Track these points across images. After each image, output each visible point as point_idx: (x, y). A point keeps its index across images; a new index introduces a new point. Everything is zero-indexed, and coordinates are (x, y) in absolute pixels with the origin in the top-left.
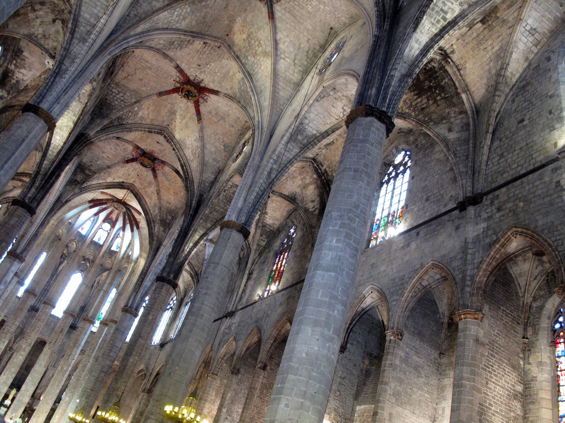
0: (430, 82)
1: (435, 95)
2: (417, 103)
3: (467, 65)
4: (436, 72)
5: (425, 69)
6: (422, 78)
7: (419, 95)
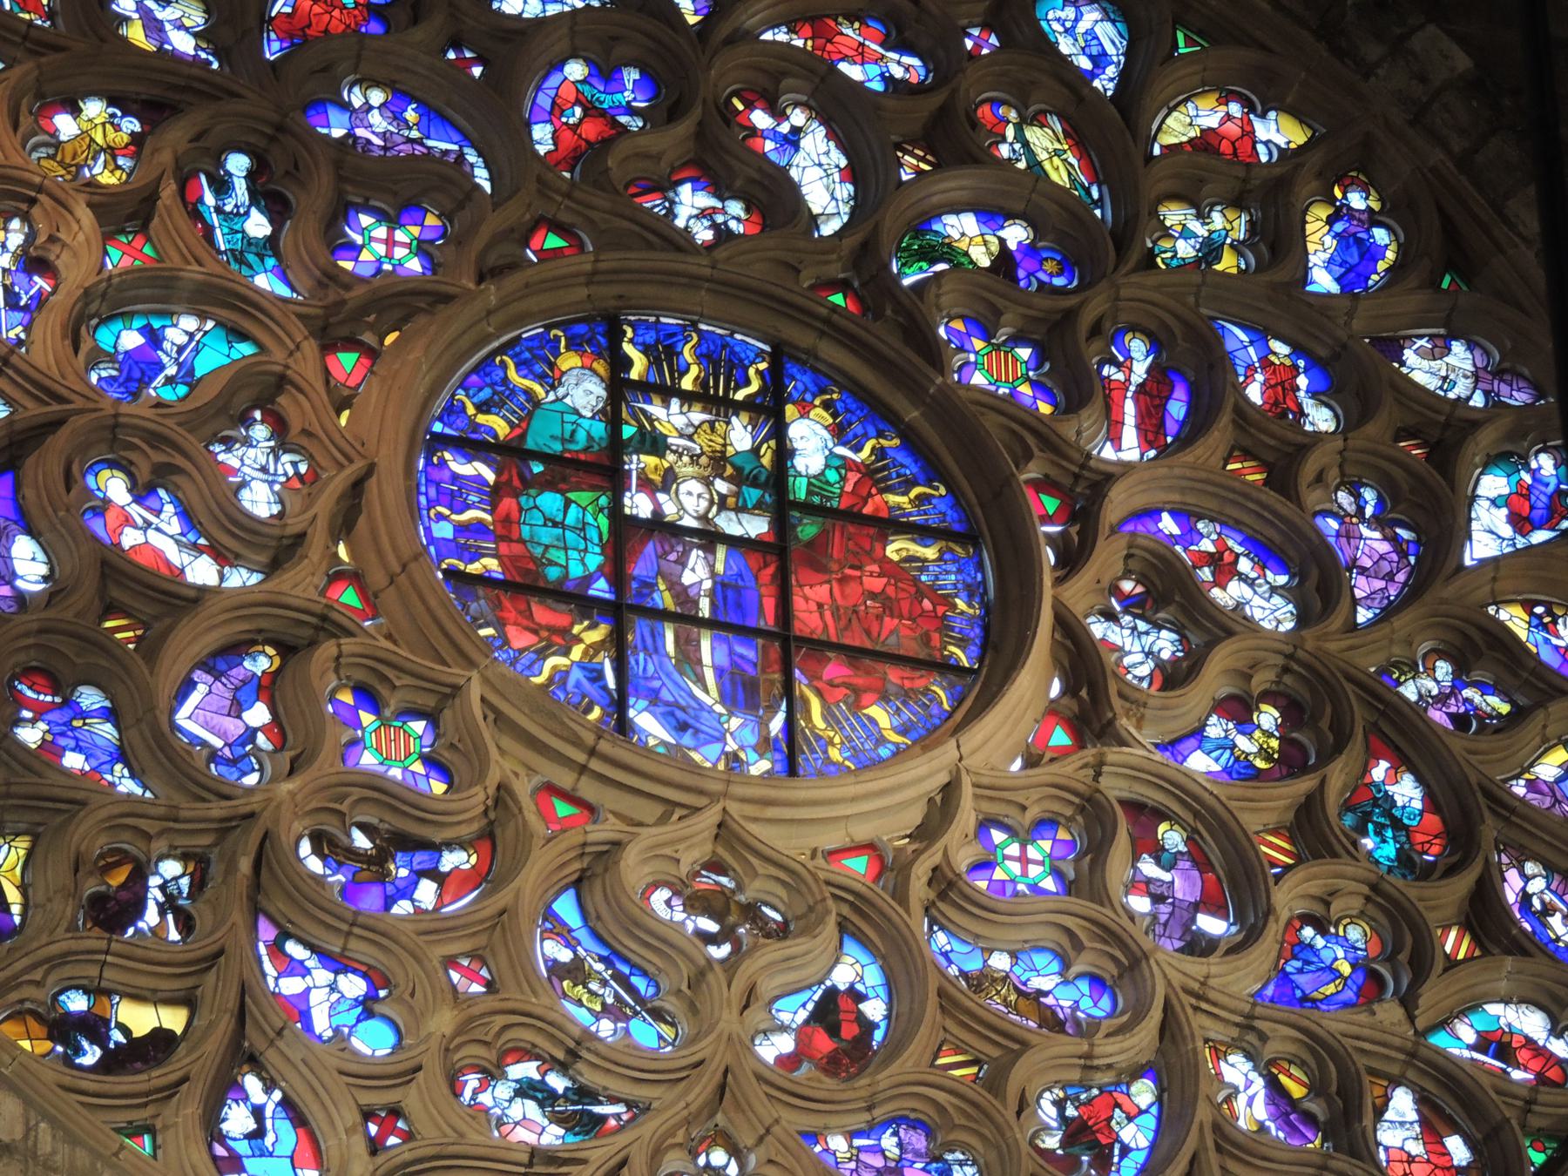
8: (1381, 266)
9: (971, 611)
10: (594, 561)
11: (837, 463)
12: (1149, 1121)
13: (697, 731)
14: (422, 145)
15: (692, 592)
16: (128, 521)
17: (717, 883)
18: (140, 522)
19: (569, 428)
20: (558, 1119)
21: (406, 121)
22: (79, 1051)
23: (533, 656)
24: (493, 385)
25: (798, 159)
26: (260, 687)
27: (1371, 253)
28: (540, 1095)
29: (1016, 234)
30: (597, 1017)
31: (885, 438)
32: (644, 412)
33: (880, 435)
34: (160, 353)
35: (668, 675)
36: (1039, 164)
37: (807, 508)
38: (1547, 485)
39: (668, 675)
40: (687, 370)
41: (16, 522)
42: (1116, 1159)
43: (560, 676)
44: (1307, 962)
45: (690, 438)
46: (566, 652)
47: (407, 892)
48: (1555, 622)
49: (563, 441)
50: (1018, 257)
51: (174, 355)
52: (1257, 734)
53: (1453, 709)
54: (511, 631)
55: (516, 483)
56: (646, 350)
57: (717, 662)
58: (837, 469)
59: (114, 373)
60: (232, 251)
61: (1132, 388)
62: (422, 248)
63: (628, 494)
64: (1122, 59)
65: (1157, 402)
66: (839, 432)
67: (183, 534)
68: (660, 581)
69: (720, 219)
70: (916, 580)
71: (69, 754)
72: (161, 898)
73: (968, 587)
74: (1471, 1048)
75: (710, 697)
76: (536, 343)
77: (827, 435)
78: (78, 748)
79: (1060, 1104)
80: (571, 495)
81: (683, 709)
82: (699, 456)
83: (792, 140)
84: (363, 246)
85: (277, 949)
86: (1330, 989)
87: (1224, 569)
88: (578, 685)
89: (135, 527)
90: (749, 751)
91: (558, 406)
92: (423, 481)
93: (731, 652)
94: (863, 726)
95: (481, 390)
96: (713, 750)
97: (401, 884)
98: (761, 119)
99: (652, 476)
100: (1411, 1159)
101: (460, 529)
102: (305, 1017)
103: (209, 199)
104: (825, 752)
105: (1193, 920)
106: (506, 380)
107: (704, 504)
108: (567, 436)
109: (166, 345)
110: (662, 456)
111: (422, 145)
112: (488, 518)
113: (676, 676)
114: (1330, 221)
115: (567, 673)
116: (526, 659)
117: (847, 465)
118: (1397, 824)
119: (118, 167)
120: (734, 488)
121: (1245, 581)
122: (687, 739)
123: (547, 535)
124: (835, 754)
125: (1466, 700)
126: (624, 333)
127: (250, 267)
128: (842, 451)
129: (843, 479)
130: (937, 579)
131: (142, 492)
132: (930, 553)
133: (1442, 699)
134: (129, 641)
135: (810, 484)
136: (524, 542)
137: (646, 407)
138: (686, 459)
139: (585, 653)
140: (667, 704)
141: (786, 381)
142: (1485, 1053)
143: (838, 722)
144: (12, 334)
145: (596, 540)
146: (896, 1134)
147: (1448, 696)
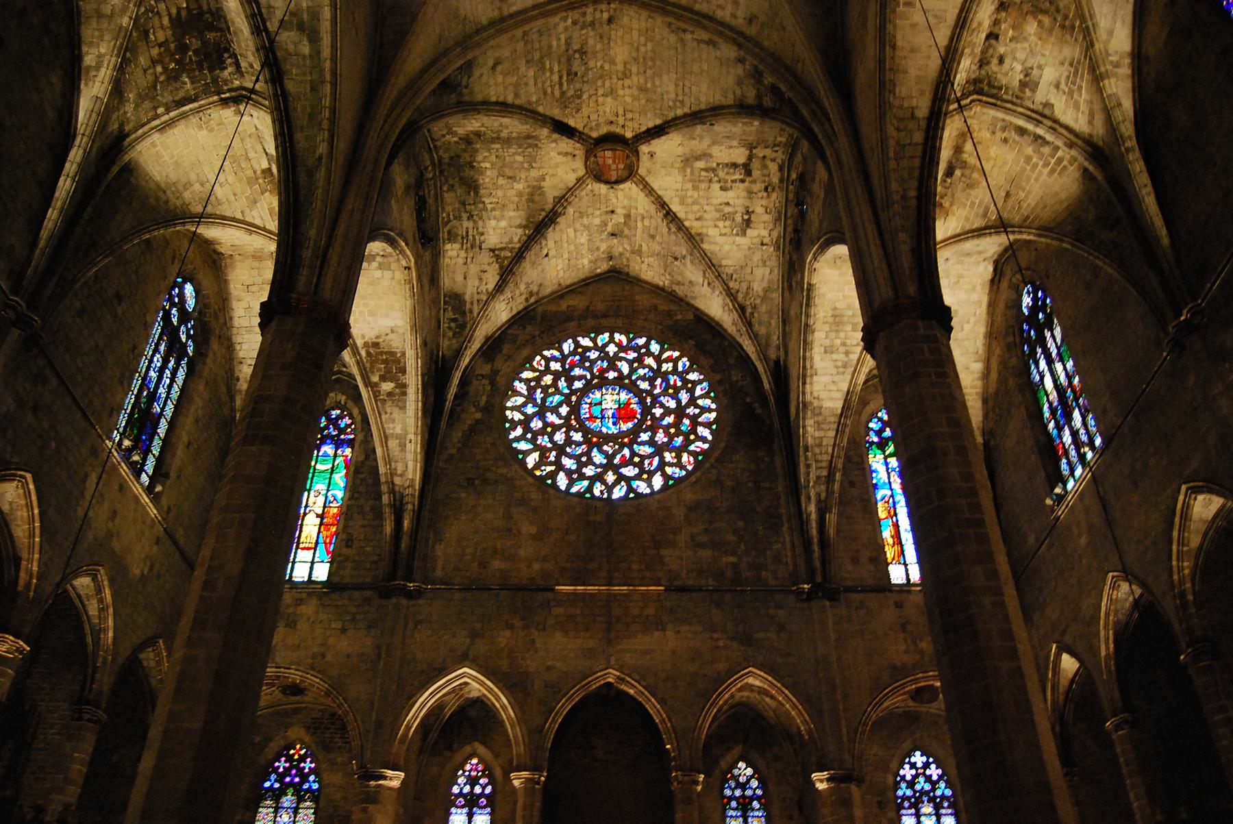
0: (196, 52)
1: (167, 59)
2: (160, 17)
3: (205, 132)
4: (211, 70)
5: (227, 50)
6: (211, 36)
7: (176, 22)
29: (647, 370)
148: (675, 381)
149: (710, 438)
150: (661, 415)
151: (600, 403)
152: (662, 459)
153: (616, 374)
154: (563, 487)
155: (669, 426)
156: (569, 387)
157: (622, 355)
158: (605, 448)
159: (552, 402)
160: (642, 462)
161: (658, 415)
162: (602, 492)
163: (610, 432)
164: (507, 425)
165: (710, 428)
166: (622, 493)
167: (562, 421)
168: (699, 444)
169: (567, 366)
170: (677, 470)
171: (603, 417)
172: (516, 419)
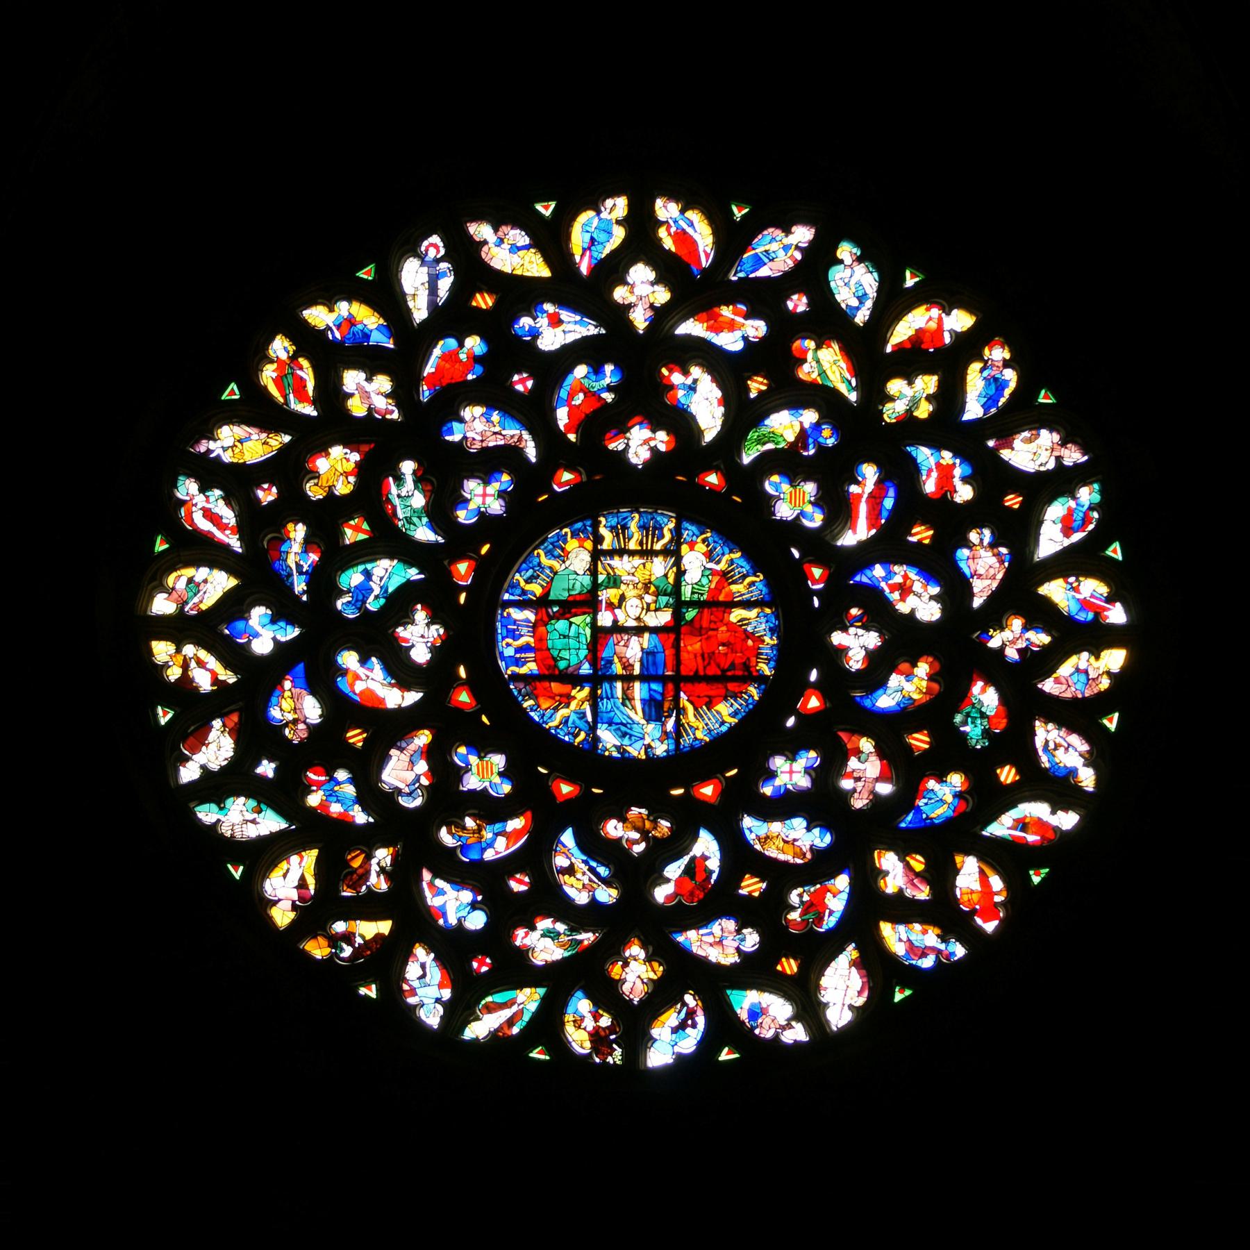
8: (1007, 392)
9: (772, 642)
10: (584, 653)
11: (707, 572)
12: (844, 896)
13: (631, 736)
14: (501, 434)
15: (631, 661)
16: (357, 677)
17: (640, 813)
18: (364, 678)
19: (571, 582)
20: (562, 946)
21: (493, 422)
22: (342, 950)
23: (552, 711)
24: (532, 568)
25: (696, 398)
26: (422, 752)
27: (1000, 385)
28: (552, 935)
29: (810, 417)
30: (580, 891)
31: (734, 553)
32: (608, 564)
33: (731, 551)
34: (371, 583)
35: (618, 708)
36: (825, 372)
37: (691, 604)
38: (1083, 506)
39: (618, 708)
40: (632, 537)
41: (305, 690)
42: (826, 918)
43: (565, 721)
44: (930, 799)
45: (633, 574)
46: (568, 707)
47: (491, 845)
48: (1079, 585)
49: (569, 590)
50: (809, 432)
51: (379, 582)
52: (916, 679)
53: (1019, 646)
54: (541, 700)
55: (546, 618)
56: (612, 529)
57: (643, 697)
58: (707, 576)
59: (350, 599)
60: (406, 518)
61: (865, 496)
62: (501, 494)
63: (600, 613)
64: (875, 294)
65: (878, 501)
66: (709, 555)
67: (384, 679)
68: (615, 657)
69: (652, 443)
70: (745, 630)
71: (333, 804)
72: (378, 869)
73: (771, 629)
74: (1009, 828)
75: (638, 717)
76: (556, 539)
77: (703, 558)
78: (338, 801)
79: (801, 896)
80: (572, 620)
81: (625, 725)
82: (637, 584)
83: (692, 388)
84: (471, 499)
85: (431, 885)
86: (939, 811)
87: (905, 590)
88: (574, 722)
89: (362, 680)
90: (657, 742)
91: (566, 572)
92: (500, 627)
93: (650, 690)
94: (714, 716)
95: (527, 571)
96: (639, 745)
97: (488, 842)
98: (677, 378)
99: (612, 601)
100: (972, 892)
101: (518, 650)
102: (444, 915)
103: (394, 490)
104: (694, 734)
105: (874, 787)
106: (539, 564)
107: (639, 610)
108: (571, 587)
109: (374, 578)
110: (619, 588)
111: (501, 434)
112: (532, 640)
113: (622, 707)
114: (982, 371)
115: (569, 717)
116: (549, 712)
117: (714, 572)
118: (983, 715)
119: (349, 483)
120: (655, 598)
121: (916, 595)
122: (626, 741)
123: (559, 643)
124: (699, 735)
125: (1027, 639)
126: (600, 522)
127: (415, 525)
128: (711, 565)
129: (710, 581)
130: (755, 627)
131: (363, 661)
132: (753, 614)
133: (1013, 642)
134: (359, 741)
135: (693, 588)
136: (549, 650)
137: (611, 562)
138: (631, 587)
139: (578, 704)
140: (617, 724)
141: (683, 531)
142: (1016, 829)
143: (702, 716)
144: (300, 589)
145: (584, 642)
146: (720, 924)
147: (1018, 639)
148: (945, 473)
149: (1087, 778)
150: (872, 656)
151: (588, 602)
152: (866, 881)
153: (662, 440)
154: (432, 1017)
155: (908, 716)
156: (439, 513)
157: (691, 328)
158: (613, 829)
159: (363, 591)
160: (774, 903)
161: (856, 661)
162: (598, 1038)
163: (636, 751)
164: (164, 716)
165: (1092, 733)
166: (689, 1042)
167: (413, 697)
168: (1038, 810)
169: (425, 393)
170: (931, 938)
171: (599, 677)
172: (203, 681)
